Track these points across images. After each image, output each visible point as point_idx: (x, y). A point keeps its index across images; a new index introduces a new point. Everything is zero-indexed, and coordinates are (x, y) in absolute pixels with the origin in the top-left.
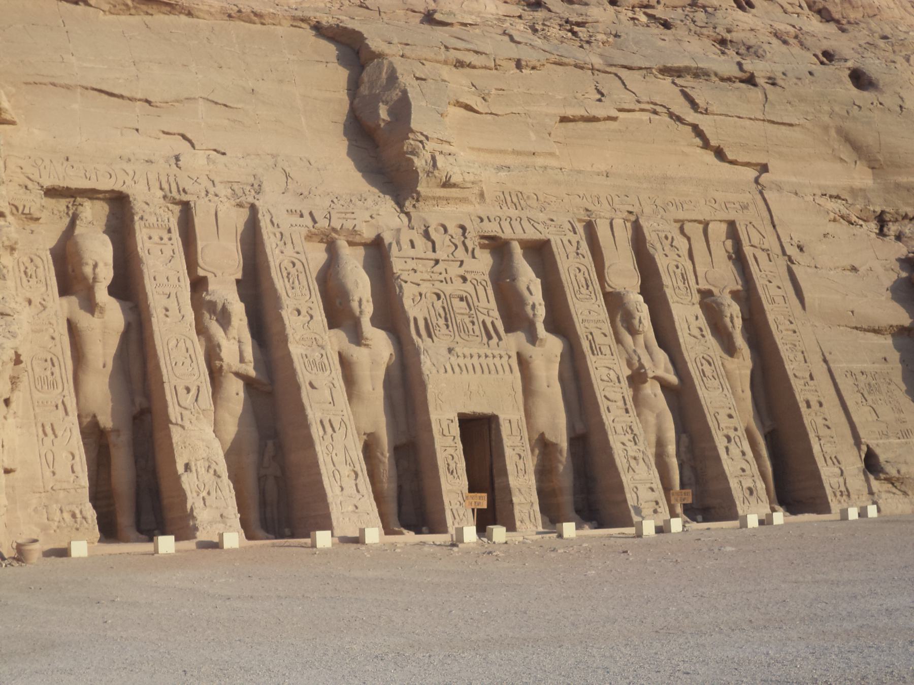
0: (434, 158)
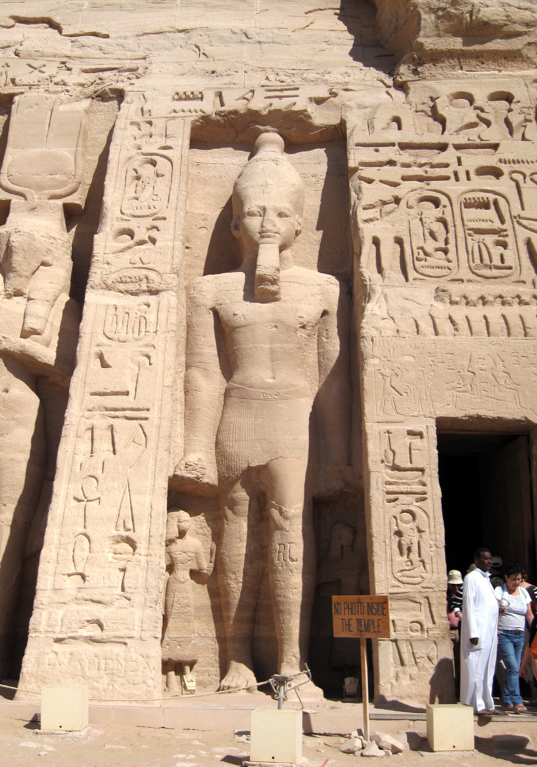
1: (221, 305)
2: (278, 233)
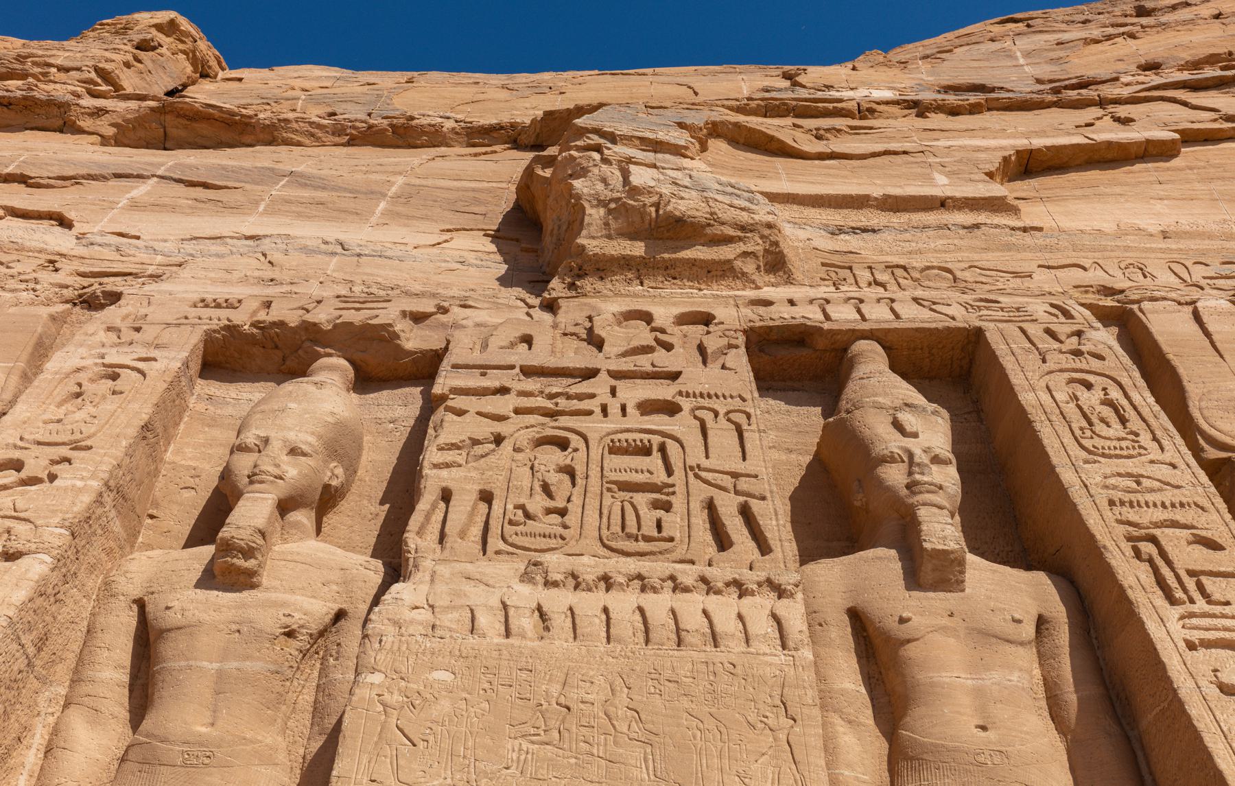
0: (626, 175)
1: (153, 593)
2: (281, 478)
